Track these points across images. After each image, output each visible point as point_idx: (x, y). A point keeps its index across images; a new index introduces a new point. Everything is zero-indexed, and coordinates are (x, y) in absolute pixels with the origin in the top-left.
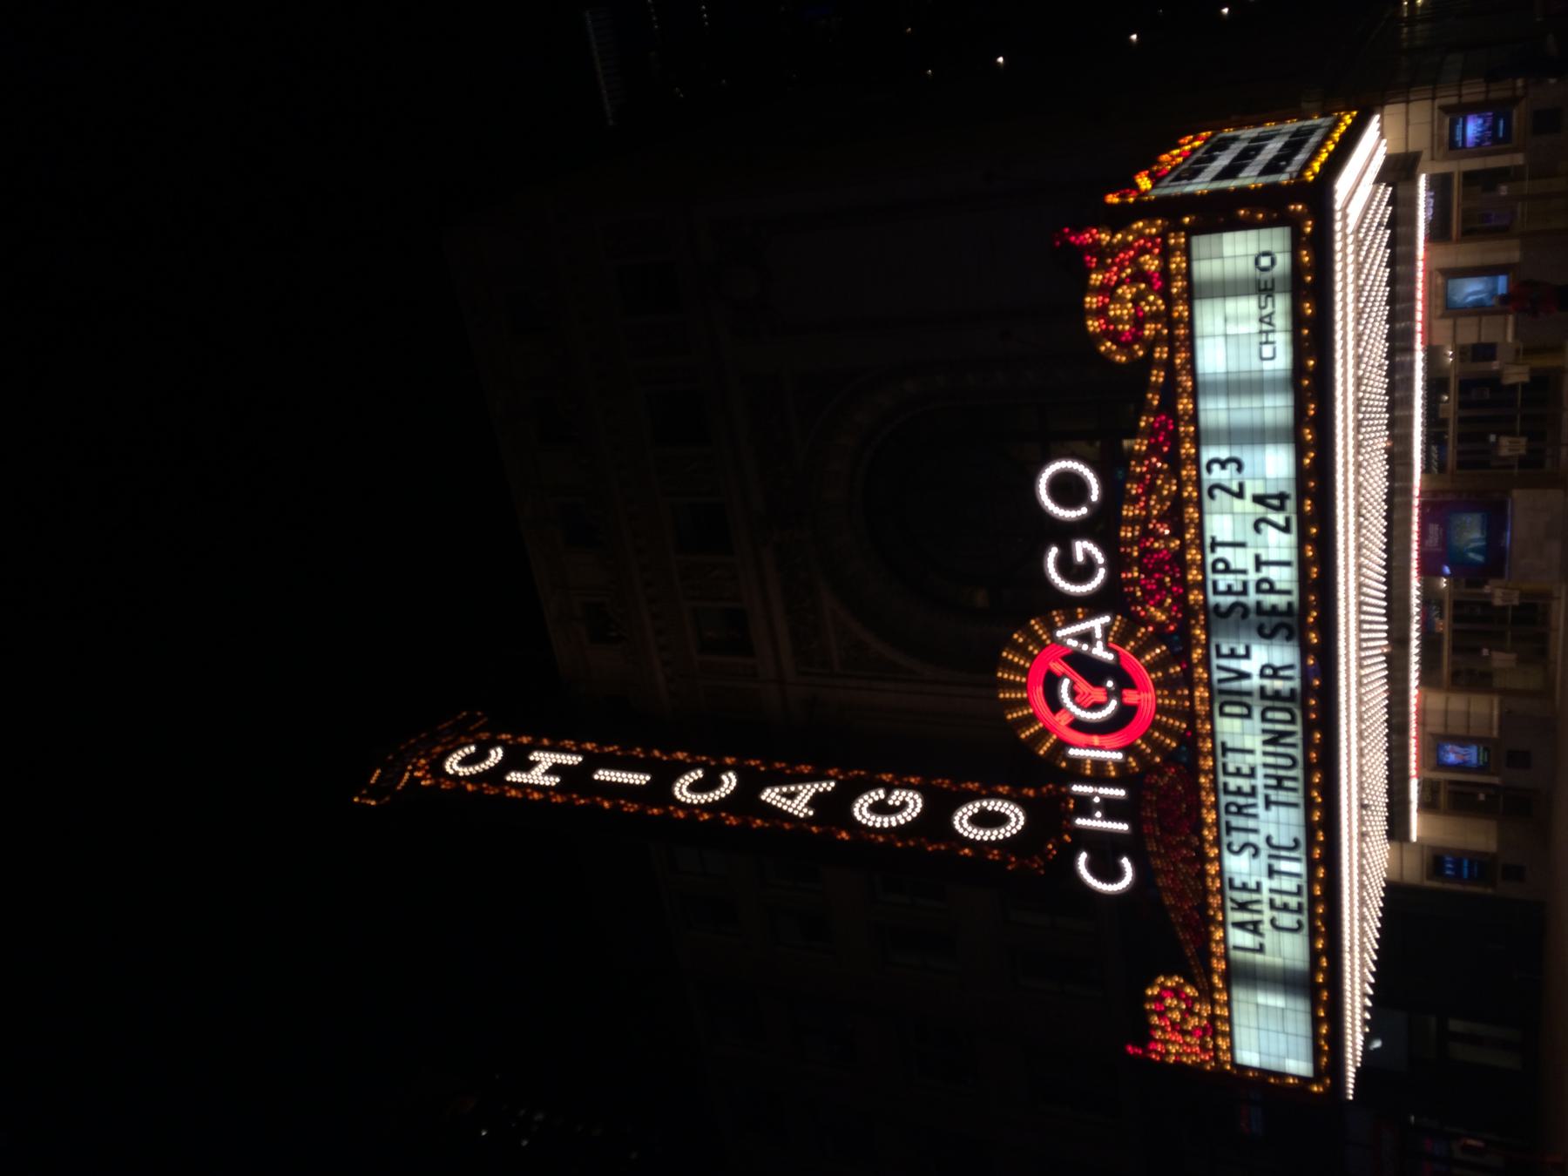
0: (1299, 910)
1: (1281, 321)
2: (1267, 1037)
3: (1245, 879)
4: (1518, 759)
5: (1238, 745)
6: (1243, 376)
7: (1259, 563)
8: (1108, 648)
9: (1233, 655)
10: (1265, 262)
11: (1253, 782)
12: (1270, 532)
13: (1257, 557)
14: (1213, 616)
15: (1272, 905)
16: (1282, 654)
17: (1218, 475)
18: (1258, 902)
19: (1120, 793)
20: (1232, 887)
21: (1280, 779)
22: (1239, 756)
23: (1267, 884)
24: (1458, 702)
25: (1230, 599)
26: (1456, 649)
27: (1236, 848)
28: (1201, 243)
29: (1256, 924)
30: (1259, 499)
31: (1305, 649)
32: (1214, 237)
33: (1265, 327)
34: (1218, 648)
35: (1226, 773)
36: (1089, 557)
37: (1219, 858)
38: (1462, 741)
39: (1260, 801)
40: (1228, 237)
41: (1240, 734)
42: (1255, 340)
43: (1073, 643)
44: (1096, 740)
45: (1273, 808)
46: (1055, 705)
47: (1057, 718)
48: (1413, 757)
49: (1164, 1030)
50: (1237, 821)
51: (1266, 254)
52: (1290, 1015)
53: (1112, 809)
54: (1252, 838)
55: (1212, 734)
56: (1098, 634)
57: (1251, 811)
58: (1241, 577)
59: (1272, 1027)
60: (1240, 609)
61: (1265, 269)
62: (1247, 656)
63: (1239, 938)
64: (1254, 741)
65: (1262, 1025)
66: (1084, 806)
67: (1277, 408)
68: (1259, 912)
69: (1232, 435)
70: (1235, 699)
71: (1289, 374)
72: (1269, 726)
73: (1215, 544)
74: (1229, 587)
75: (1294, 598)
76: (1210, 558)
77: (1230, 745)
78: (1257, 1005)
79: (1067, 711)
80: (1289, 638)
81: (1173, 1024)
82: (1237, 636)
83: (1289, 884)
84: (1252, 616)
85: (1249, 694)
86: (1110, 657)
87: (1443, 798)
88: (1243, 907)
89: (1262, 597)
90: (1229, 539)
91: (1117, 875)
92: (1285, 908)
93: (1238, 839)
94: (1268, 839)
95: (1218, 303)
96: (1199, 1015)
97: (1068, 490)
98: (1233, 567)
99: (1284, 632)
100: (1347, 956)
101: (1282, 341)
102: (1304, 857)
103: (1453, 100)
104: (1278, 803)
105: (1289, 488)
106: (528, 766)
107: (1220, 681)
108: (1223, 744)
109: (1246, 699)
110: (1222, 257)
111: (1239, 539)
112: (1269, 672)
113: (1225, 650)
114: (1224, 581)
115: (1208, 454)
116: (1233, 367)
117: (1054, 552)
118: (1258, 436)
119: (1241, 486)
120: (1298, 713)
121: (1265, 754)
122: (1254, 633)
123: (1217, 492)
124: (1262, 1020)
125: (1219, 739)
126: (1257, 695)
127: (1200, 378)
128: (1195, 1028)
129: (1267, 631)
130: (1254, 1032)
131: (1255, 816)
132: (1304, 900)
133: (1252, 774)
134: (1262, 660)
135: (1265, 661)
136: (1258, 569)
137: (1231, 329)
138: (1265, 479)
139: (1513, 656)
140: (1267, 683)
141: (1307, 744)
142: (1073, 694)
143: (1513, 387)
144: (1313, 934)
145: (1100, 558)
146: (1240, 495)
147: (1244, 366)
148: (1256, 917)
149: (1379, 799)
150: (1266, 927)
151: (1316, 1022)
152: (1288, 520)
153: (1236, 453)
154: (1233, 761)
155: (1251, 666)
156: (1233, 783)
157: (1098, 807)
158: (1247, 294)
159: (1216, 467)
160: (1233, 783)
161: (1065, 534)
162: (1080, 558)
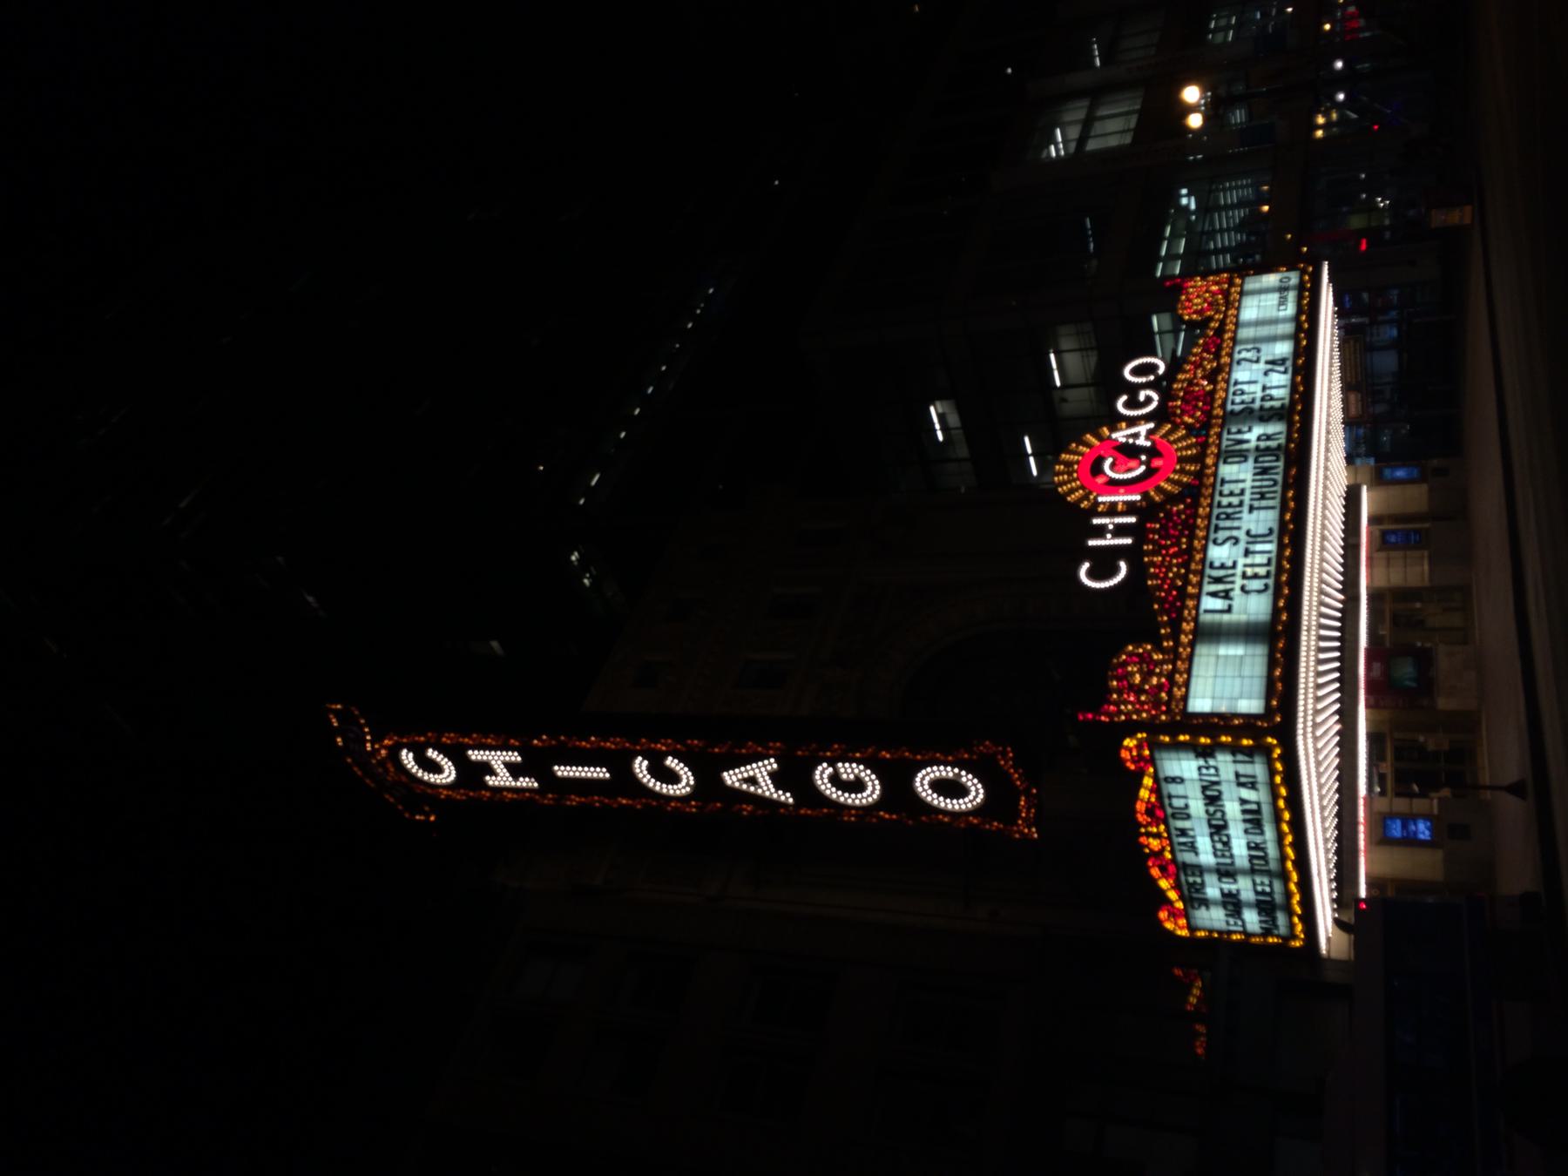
7: (1264, 388)
9: (1239, 432)
15: (1244, 576)
20: (1212, 566)
23: (1241, 561)
30: (1267, 362)
45: (1255, 513)
48: (1362, 836)
50: (1228, 524)
52: (1248, 660)
54: (1235, 533)
59: (1229, 672)
66: (1100, 532)
76: (1232, 389)
78: (1218, 657)
83: (1259, 559)
88: (1218, 580)
92: (1256, 576)
93: (1222, 535)
94: (1248, 533)
104: (1259, 508)
124: (1220, 668)
132: (1272, 568)
133: (1242, 492)
144: (1277, 595)
146: (1257, 361)
148: (1229, 586)
150: (1237, 593)
151: (1272, 663)
154: (1226, 489)
160: (1225, 501)
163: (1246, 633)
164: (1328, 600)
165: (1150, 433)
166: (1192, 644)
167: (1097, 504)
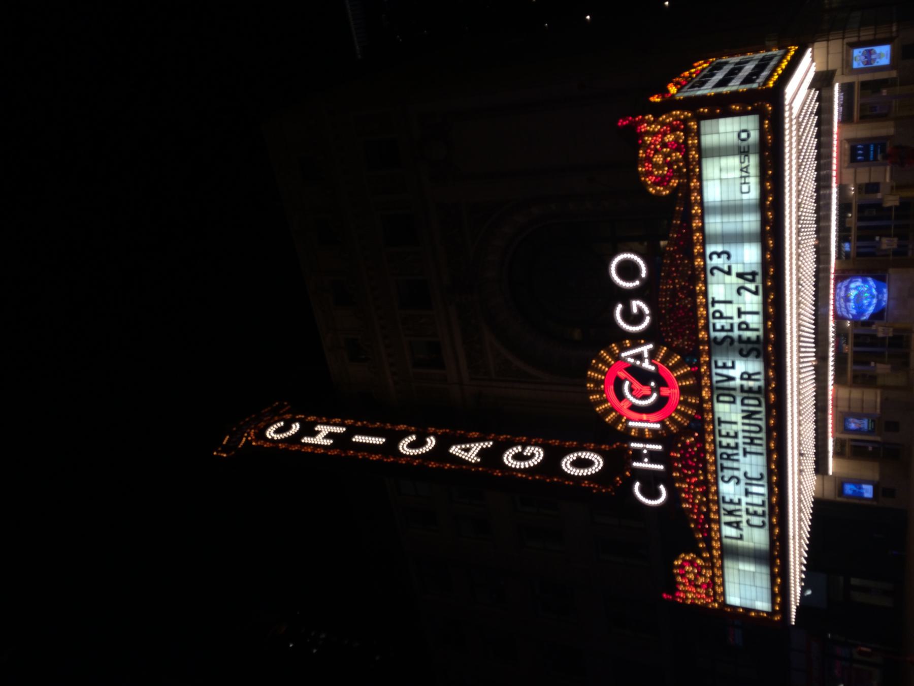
0: (763, 515)
1: (753, 170)
2: (745, 589)
3: (732, 497)
4: (892, 426)
5: (727, 419)
6: (731, 203)
7: (740, 313)
8: (651, 363)
9: (725, 366)
10: (744, 135)
11: (736, 440)
12: (747, 295)
13: (739, 310)
14: (713, 344)
15: (748, 512)
16: (754, 366)
17: (716, 261)
18: (739, 510)
19: (659, 447)
20: (724, 502)
21: (752, 439)
22: (728, 426)
23: (744, 500)
24: (856, 394)
25: (723, 334)
26: (855, 362)
27: (726, 479)
28: (706, 125)
29: (738, 523)
30: (740, 275)
31: (767, 367)
32: (714, 121)
33: (744, 174)
34: (716, 362)
35: (720, 435)
36: (640, 309)
37: (716, 484)
38: (859, 416)
39: (741, 451)
40: (722, 121)
41: (729, 412)
42: (738, 182)
43: (631, 360)
44: (645, 417)
45: (748, 456)
46: (621, 397)
47: (622, 404)
48: (830, 426)
49: (684, 585)
50: (727, 464)
51: (744, 131)
52: (758, 575)
53: (654, 457)
54: (736, 473)
55: (712, 410)
56: (646, 355)
57: (735, 457)
58: (730, 321)
59: (748, 582)
60: (729, 340)
61: (744, 140)
62: (733, 367)
63: (728, 531)
64: (737, 417)
65: (742, 581)
66: (638, 455)
67: (751, 222)
68: (740, 516)
69: (725, 238)
70: (726, 392)
71: (758, 202)
72: (746, 408)
73: (714, 302)
74: (723, 327)
75: (761, 333)
76: (711, 310)
77: (723, 419)
79: (628, 400)
80: (757, 357)
81: (690, 581)
82: (727, 356)
83: (757, 500)
84: (736, 344)
85: (734, 389)
86: (653, 368)
87: (847, 449)
88: (730, 513)
89: (741, 333)
90: (722, 298)
91: (657, 495)
93: (727, 474)
94: (745, 474)
95: (716, 160)
96: (705, 576)
97: (628, 270)
98: (725, 315)
99: (755, 353)
100: (791, 542)
101: (753, 181)
102: (766, 484)
103: (854, 39)
104: (751, 453)
105: (758, 269)
106: (314, 434)
107: (718, 382)
108: (719, 419)
109: (732, 392)
110: (718, 133)
111: (728, 299)
112: (746, 376)
113: (720, 364)
114: (719, 323)
115: (710, 249)
116: (725, 198)
117: (620, 307)
118: (740, 238)
119: (730, 268)
120: (763, 400)
121: (744, 424)
122: (737, 354)
123: (715, 271)
125: (717, 416)
126: (739, 390)
127: (706, 205)
128: (703, 583)
129: (745, 353)
130: (737, 586)
131: (737, 460)
132: (766, 509)
133: (736, 436)
134: (742, 369)
135: (743, 370)
136: (739, 316)
137: (724, 176)
138: (744, 263)
139: (889, 366)
140: (745, 383)
141: (768, 416)
142: (631, 390)
143: (890, 208)
145: (647, 310)
146: (729, 273)
147: (732, 197)
148: (738, 519)
149: (810, 450)
150: (744, 525)
151: (773, 577)
152: (757, 287)
153: (727, 249)
154: (725, 429)
155: (736, 373)
156: (725, 441)
157: (646, 456)
158: (733, 155)
159: (715, 257)
160: (725, 441)
161: (626, 296)
162: (635, 310)
163: (754, 556)
164: (804, 334)
165: (653, 355)
166: (721, 557)
167: (629, 429)
